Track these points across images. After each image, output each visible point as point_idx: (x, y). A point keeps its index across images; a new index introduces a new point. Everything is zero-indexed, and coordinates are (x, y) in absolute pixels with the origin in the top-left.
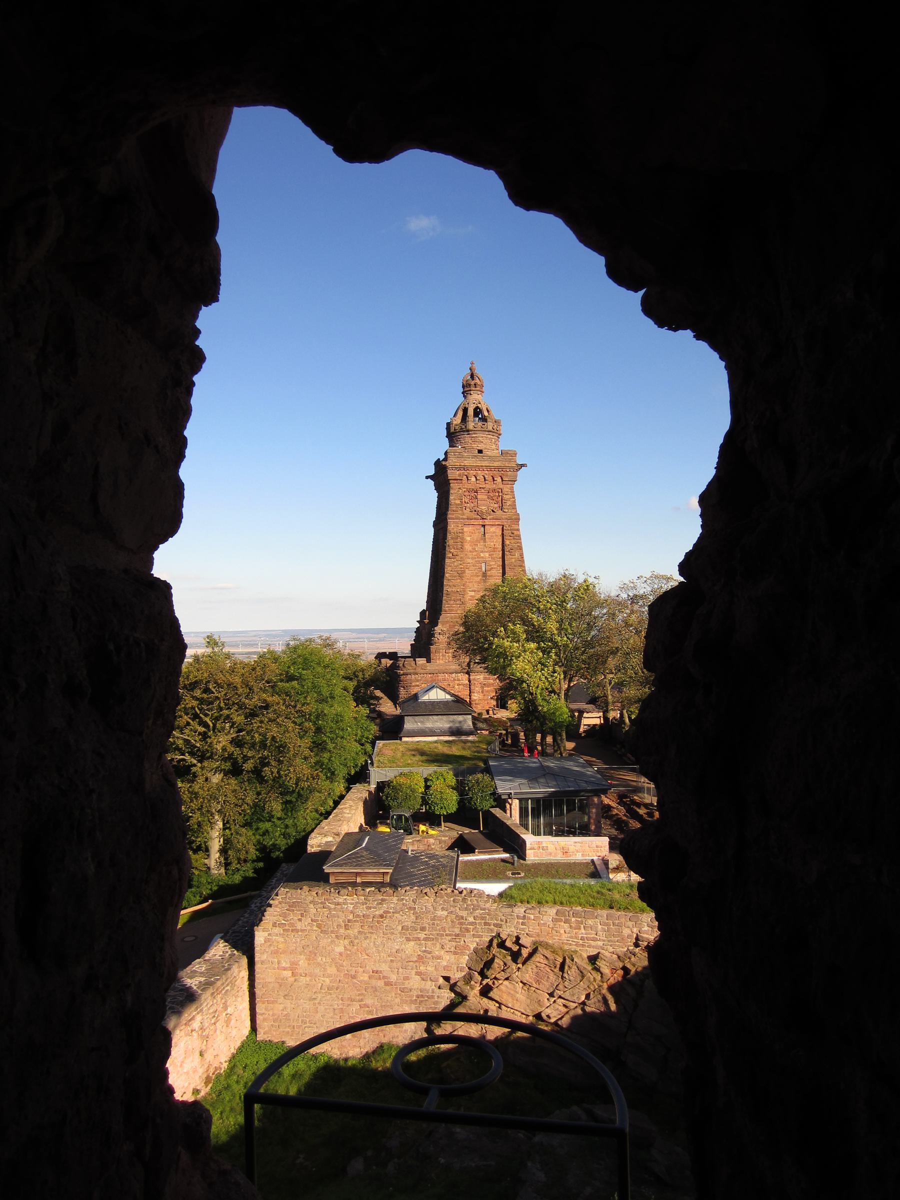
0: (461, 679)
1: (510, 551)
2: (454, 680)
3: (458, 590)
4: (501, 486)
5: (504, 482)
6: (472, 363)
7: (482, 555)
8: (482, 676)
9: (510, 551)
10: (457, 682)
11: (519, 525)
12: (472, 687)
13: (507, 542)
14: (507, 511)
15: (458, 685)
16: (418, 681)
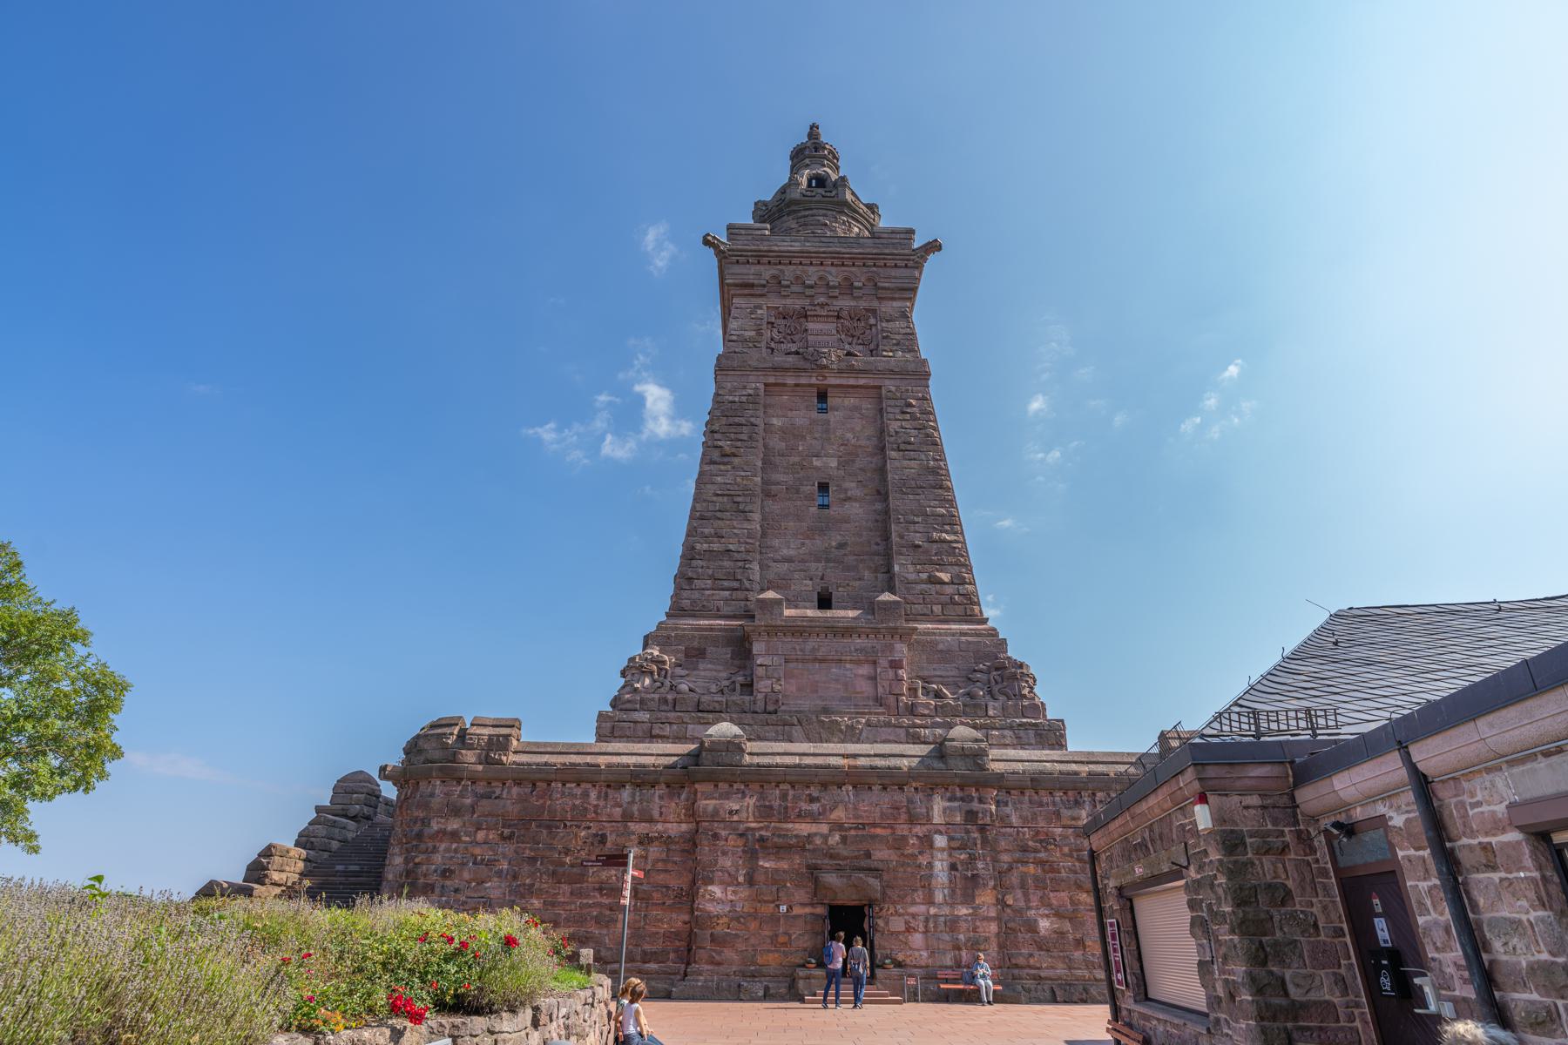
0: (656, 814)
1: (902, 447)
2: (627, 817)
3: (731, 547)
4: (875, 304)
5: (881, 294)
6: (814, 127)
7: (817, 462)
8: (751, 801)
9: (902, 447)
10: (639, 828)
11: (928, 387)
12: (704, 852)
13: (894, 426)
14: (891, 354)
15: (645, 841)
16: (456, 811)
